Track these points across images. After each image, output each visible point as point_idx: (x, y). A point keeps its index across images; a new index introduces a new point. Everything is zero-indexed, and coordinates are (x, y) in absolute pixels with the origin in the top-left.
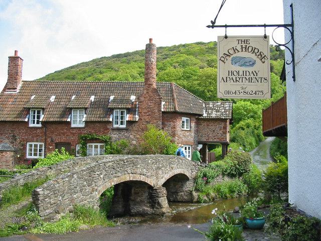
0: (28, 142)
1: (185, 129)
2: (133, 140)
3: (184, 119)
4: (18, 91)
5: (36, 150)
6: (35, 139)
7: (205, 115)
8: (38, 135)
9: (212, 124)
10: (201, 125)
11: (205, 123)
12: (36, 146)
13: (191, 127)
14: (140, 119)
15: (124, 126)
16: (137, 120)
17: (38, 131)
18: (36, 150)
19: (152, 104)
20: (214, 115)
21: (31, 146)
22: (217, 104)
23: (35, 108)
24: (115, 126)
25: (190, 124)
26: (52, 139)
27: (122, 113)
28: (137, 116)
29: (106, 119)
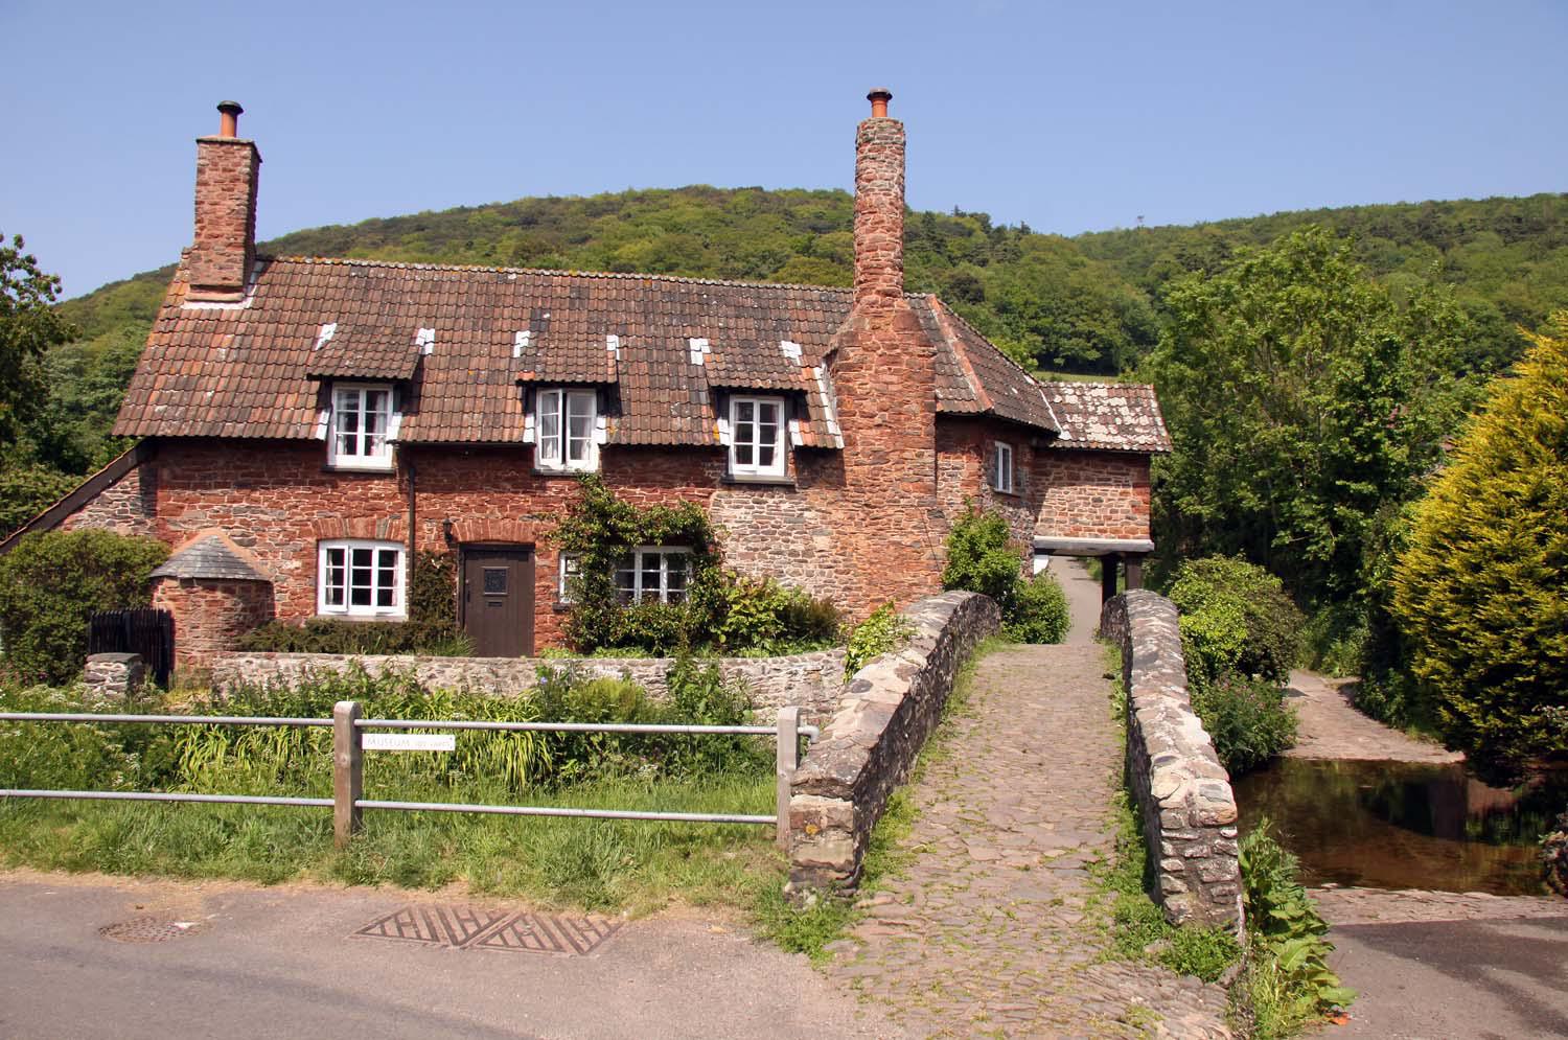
0: (328, 539)
1: (1000, 489)
2: (816, 530)
3: (1000, 445)
4: (249, 303)
5: (362, 577)
6: (360, 523)
7: (1065, 436)
8: (374, 509)
9: (1090, 472)
10: (1047, 474)
11: (1063, 471)
12: (362, 557)
13: (1017, 484)
14: (850, 442)
15: (777, 470)
16: (840, 444)
17: (376, 487)
18: (362, 577)
19: (894, 379)
20: (1100, 435)
21: (337, 557)
22: (1094, 393)
23: (353, 379)
24: (738, 470)
25: (1015, 470)
26: (448, 525)
27: (767, 414)
28: (833, 428)
29: (707, 440)
